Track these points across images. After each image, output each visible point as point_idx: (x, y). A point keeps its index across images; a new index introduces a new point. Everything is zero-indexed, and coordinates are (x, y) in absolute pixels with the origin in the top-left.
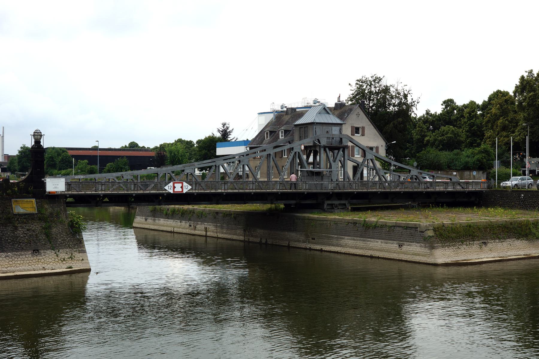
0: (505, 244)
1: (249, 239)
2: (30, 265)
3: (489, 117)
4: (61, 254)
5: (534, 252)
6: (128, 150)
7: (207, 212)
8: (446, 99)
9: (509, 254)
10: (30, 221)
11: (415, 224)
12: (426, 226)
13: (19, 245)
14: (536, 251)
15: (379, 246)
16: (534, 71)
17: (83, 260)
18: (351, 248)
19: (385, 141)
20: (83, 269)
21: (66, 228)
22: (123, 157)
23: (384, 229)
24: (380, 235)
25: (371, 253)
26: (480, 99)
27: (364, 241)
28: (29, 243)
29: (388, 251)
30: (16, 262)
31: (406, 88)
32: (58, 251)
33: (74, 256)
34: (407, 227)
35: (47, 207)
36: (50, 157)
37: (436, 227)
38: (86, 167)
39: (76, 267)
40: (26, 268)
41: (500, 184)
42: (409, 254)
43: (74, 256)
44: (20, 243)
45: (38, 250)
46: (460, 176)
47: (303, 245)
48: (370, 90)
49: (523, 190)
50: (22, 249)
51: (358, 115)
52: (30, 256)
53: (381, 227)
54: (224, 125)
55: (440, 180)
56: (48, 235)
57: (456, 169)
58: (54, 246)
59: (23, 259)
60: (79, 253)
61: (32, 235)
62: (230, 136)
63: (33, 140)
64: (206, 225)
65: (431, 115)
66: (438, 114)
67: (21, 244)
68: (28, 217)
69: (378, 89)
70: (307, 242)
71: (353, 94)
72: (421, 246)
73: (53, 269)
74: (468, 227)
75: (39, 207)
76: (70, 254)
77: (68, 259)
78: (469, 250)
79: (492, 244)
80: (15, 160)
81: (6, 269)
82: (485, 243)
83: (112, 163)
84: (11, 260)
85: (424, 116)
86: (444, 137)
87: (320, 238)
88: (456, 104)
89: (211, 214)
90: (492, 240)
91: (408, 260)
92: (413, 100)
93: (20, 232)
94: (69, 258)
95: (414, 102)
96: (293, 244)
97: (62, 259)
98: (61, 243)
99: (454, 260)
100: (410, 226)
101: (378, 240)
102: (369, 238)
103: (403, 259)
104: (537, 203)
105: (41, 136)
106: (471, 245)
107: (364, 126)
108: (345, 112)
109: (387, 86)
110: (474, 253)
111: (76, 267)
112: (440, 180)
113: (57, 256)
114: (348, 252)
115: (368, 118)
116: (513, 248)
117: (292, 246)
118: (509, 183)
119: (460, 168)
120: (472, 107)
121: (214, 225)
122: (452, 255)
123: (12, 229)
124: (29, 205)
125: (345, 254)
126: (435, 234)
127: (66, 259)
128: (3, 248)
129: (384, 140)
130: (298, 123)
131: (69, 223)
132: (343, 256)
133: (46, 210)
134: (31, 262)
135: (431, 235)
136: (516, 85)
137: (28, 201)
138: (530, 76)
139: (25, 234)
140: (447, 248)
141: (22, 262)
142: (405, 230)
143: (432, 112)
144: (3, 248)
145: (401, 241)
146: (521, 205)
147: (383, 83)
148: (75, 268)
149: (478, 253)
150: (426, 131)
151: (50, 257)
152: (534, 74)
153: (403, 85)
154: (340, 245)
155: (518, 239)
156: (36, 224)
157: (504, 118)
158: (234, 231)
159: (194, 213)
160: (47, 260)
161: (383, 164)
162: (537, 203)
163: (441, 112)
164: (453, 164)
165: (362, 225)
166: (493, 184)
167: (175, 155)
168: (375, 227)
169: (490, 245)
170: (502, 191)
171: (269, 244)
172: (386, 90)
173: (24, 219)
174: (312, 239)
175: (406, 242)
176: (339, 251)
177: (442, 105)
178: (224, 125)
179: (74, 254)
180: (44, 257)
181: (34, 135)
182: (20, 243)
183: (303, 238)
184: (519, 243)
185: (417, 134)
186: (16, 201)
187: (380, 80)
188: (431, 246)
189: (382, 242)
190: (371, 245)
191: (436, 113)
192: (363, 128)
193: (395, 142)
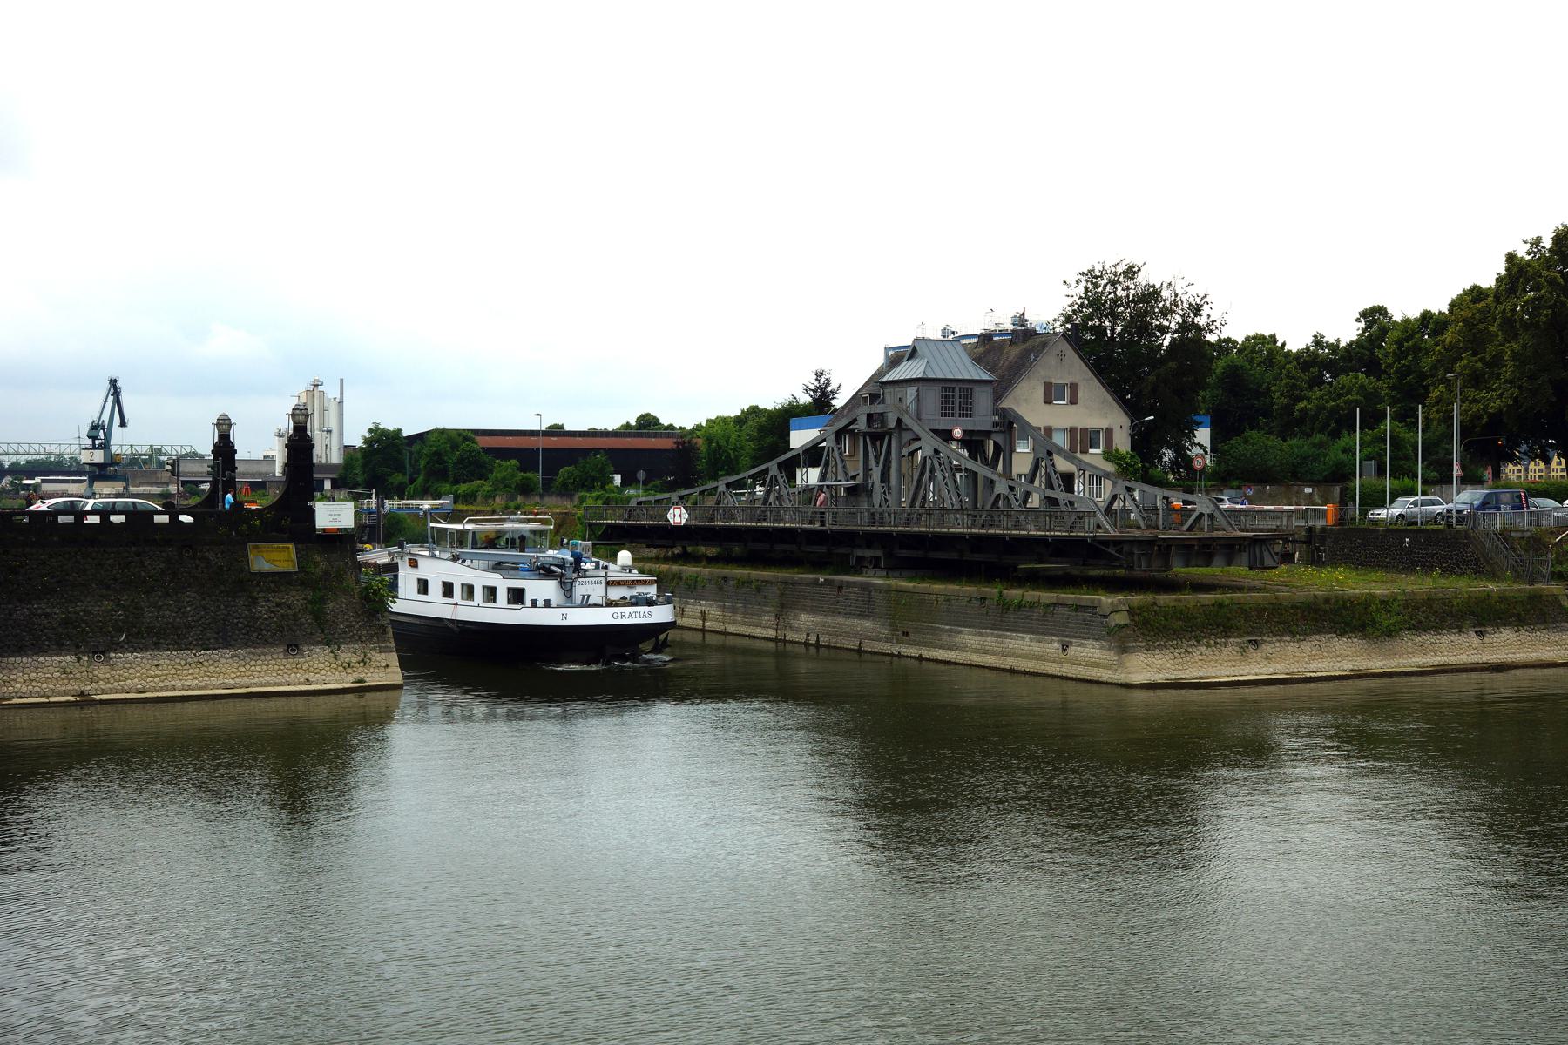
0: (1306, 646)
1: (785, 636)
2: (279, 675)
3: (1440, 353)
4: (344, 655)
5: (1380, 664)
7: (706, 577)
9: (1313, 666)
10: (283, 588)
11: (1093, 601)
12: (1112, 602)
13: (259, 635)
14: (1384, 663)
15: (1026, 648)
17: (387, 666)
18: (975, 652)
19: (1129, 416)
20: (387, 685)
21: (355, 603)
23: (1036, 610)
24: (1029, 623)
25: (1011, 664)
26: (1439, 304)
27: (999, 636)
28: (279, 630)
29: (1043, 658)
30: (253, 668)
31: (1192, 291)
32: (336, 647)
33: (370, 659)
34: (1077, 608)
35: (318, 559)
36: (435, 453)
37: (1136, 605)
40: (272, 679)
41: (1366, 514)
42: (1081, 665)
43: (370, 659)
44: (262, 630)
45: (296, 646)
46: (1321, 497)
47: (886, 648)
48: (1112, 295)
49: (1409, 528)
50: (266, 643)
51: (1061, 356)
52: (281, 656)
53: (1030, 607)
55: (1272, 507)
56: (319, 617)
57: (1312, 481)
58: (330, 637)
59: (266, 662)
60: (380, 652)
61: (287, 615)
63: (291, 423)
64: (704, 605)
65: (1328, 345)
66: (1289, 351)
67: (264, 632)
68: (279, 580)
69: (1132, 292)
70: (894, 641)
72: (1102, 647)
73: (325, 684)
74: (1216, 608)
75: (302, 558)
76: (362, 655)
77: (357, 665)
78: (1215, 658)
79: (1273, 646)
80: (357, 460)
81: (232, 682)
82: (1255, 643)
84: (244, 663)
85: (1308, 348)
86: (1341, 402)
87: (919, 632)
88: (1394, 319)
89: (713, 582)
90: (1275, 636)
91: (1079, 676)
92: (1211, 319)
93: (262, 609)
95: (1213, 322)
96: (869, 645)
97: (345, 665)
98: (345, 632)
99: (1173, 677)
100: (1082, 604)
101: (1024, 635)
102: (1008, 630)
103: (1070, 675)
104: (1437, 558)
105: (307, 416)
106: (1218, 646)
107: (1076, 381)
109: (1154, 286)
110: (1226, 664)
112: (1272, 507)
113: (335, 657)
114: (969, 662)
115: (1088, 366)
116: (1325, 654)
117: (866, 649)
118: (1382, 513)
119: (1321, 478)
120: (1406, 327)
121: (719, 606)
122: (1168, 666)
123: (246, 603)
124: (283, 556)
125: (933, 660)
126: (1132, 620)
127: (352, 664)
128: (229, 639)
129: (1127, 413)
130: (891, 379)
131: (361, 593)
132: (941, 667)
133: (316, 564)
134: (282, 668)
135: (1122, 623)
136: (1498, 274)
137: (279, 548)
138: (1535, 253)
139: (272, 612)
140: (1157, 651)
141: (265, 667)
142: (1074, 614)
143: (1330, 338)
144: (229, 639)
145: (1066, 637)
146: (1403, 563)
147: (1142, 278)
148: (372, 681)
149: (1234, 663)
151: (321, 659)
152: (1544, 248)
154: (954, 645)
155: (1342, 635)
156: (294, 593)
158: (756, 617)
159: (680, 578)
160: (315, 666)
161: (1123, 469)
162: (1437, 558)
163: (1354, 338)
164: (1306, 469)
165: (995, 603)
166: (1351, 512)
168: (1020, 607)
169: (1267, 648)
170: (1366, 530)
171: (824, 646)
172: (1151, 295)
173: (272, 582)
174: (904, 633)
175: (1076, 637)
176: (953, 660)
177: (1358, 320)
180: (308, 658)
181: (293, 415)
182: (262, 630)
183: (885, 632)
184: (1340, 644)
185: (1282, 395)
186: (257, 547)
187: (1135, 273)
188: (1120, 647)
189: (1031, 640)
190: (1011, 646)
191: (1338, 340)
192: (1074, 387)
193: (1152, 417)
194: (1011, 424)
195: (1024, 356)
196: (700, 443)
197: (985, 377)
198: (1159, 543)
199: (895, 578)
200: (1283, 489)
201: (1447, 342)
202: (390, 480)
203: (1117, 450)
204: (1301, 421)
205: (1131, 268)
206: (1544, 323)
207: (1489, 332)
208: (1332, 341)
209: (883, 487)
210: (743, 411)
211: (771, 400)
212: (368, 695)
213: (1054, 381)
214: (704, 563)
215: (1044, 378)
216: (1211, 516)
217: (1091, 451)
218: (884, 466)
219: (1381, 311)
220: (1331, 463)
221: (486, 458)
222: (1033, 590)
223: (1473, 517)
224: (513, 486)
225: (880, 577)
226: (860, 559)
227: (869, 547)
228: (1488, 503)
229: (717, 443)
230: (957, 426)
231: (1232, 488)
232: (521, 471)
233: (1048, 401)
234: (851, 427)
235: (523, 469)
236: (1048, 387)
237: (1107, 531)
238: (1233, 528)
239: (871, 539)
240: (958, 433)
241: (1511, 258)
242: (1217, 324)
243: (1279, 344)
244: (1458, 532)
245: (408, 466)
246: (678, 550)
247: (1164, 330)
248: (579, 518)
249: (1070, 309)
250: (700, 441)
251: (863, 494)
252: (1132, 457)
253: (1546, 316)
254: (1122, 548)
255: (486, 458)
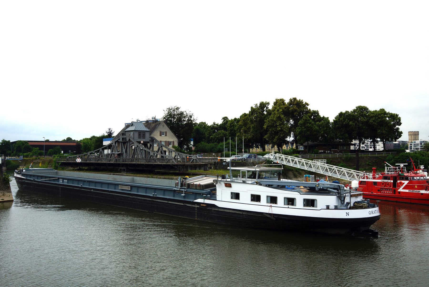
3: (238, 126)
6: (65, 142)
8: (224, 117)
16: (258, 104)
17: (9, 196)
20: (9, 200)
22: (58, 146)
26: (238, 117)
31: (190, 113)
36: (18, 146)
38: (38, 151)
39: (6, 199)
46: (216, 155)
48: (174, 113)
51: (163, 126)
54: (110, 129)
60: (8, 193)
62: (112, 135)
65: (216, 124)
69: (178, 113)
71: (165, 115)
77: (2, 196)
83: (52, 149)
85: (212, 125)
88: (229, 119)
92: (194, 119)
94: (2, 195)
108: (157, 124)
111: (6, 199)
119: (216, 152)
138: (256, 107)
143: (216, 123)
147: (180, 110)
150: (212, 133)
153: (189, 111)
157: (245, 127)
163: (221, 123)
167: (86, 145)
172: (182, 113)
177: (222, 119)
178: (110, 129)
179: (5, 193)
187: (179, 109)
191: (218, 123)
192: (166, 132)
194: (153, 140)
195: (156, 126)
196: (82, 144)
197: (148, 130)
198: (186, 165)
199: (129, 173)
200: (209, 154)
201: (240, 124)
202: (7, 152)
203: (175, 146)
204: (211, 140)
205: (178, 108)
206: (258, 121)
207: (248, 122)
208: (217, 124)
209: (126, 154)
210: (91, 137)
211: (98, 134)
212: (5, 203)
213: (162, 131)
214: (85, 171)
215: (160, 130)
216: (196, 160)
217: (170, 146)
218: (126, 149)
219: (226, 118)
220: (218, 148)
221: (31, 147)
222: (159, 176)
223: (247, 159)
224: (38, 153)
225: (125, 173)
226: (121, 169)
227: (122, 167)
228: (250, 157)
229: (86, 144)
230: (142, 140)
231: (198, 154)
232: (40, 150)
233: (161, 135)
234: (119, 141)
235: (40, 150)
236: (161, 132)
237: (174, 163)
238: (200, 162)
239: (123, 165)
240: (142, 142)
241: (252, 108)
242: (195, 120)
243: (206, 124)
244: (244, 162)
245: (11, 149)
246: (78, 168)
247: (185, 121)
248: (54, 161)
249: (165, 116)
250: (82, 144)
251: (121, 155)
252: (178, 147)
253: (259, 119)
254: (178, 166)
255: (31, 147)
